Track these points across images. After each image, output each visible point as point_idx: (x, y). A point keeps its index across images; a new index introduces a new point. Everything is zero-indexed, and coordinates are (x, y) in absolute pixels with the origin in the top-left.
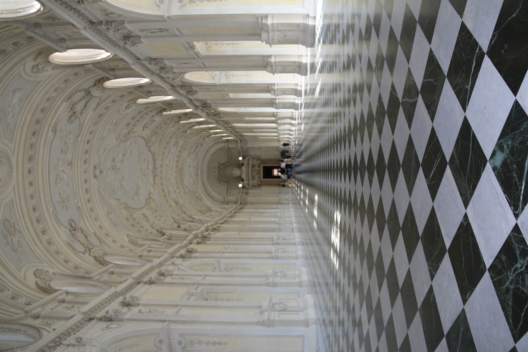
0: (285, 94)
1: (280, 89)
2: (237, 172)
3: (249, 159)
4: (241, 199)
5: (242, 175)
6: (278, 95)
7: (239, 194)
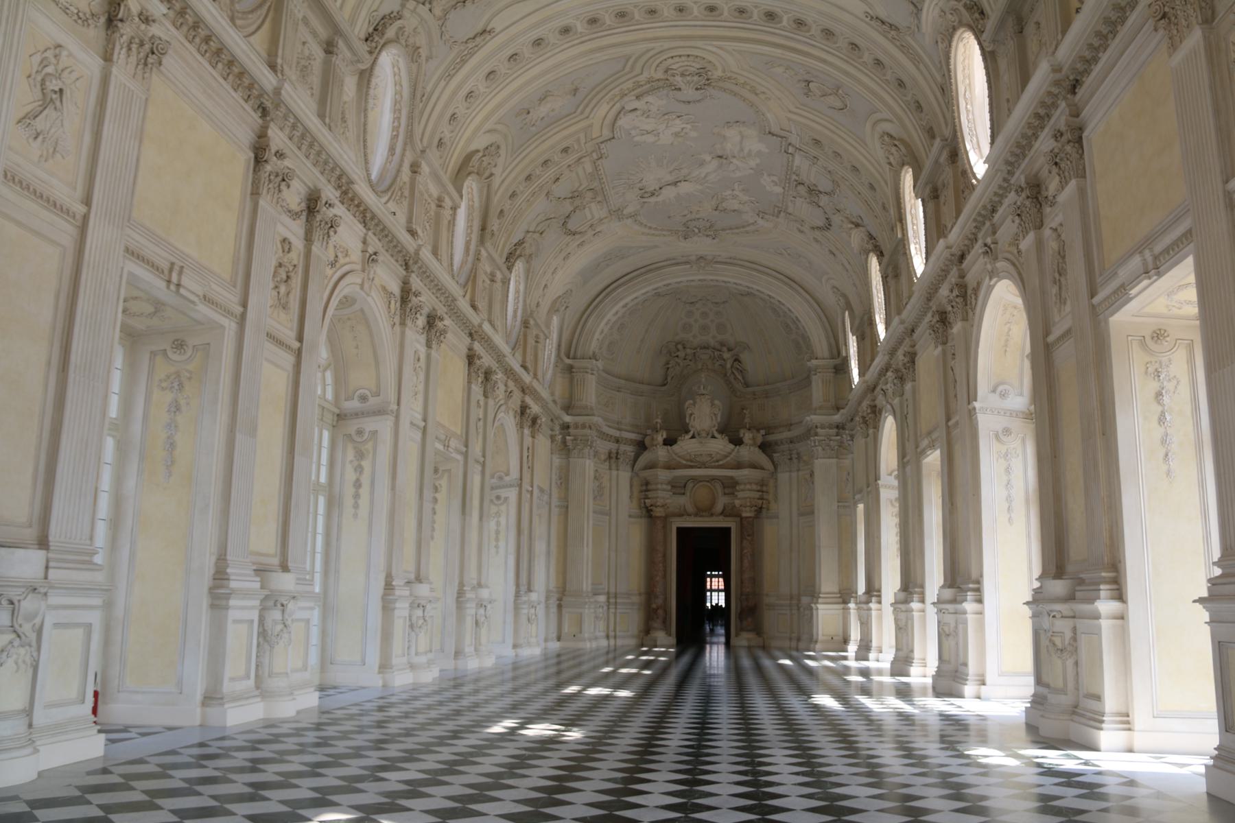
1: (965, 623)
2: (704, 415)
3: (763, 469)
4: (584, 427)
5: (693, 437)
7: (609, 426)
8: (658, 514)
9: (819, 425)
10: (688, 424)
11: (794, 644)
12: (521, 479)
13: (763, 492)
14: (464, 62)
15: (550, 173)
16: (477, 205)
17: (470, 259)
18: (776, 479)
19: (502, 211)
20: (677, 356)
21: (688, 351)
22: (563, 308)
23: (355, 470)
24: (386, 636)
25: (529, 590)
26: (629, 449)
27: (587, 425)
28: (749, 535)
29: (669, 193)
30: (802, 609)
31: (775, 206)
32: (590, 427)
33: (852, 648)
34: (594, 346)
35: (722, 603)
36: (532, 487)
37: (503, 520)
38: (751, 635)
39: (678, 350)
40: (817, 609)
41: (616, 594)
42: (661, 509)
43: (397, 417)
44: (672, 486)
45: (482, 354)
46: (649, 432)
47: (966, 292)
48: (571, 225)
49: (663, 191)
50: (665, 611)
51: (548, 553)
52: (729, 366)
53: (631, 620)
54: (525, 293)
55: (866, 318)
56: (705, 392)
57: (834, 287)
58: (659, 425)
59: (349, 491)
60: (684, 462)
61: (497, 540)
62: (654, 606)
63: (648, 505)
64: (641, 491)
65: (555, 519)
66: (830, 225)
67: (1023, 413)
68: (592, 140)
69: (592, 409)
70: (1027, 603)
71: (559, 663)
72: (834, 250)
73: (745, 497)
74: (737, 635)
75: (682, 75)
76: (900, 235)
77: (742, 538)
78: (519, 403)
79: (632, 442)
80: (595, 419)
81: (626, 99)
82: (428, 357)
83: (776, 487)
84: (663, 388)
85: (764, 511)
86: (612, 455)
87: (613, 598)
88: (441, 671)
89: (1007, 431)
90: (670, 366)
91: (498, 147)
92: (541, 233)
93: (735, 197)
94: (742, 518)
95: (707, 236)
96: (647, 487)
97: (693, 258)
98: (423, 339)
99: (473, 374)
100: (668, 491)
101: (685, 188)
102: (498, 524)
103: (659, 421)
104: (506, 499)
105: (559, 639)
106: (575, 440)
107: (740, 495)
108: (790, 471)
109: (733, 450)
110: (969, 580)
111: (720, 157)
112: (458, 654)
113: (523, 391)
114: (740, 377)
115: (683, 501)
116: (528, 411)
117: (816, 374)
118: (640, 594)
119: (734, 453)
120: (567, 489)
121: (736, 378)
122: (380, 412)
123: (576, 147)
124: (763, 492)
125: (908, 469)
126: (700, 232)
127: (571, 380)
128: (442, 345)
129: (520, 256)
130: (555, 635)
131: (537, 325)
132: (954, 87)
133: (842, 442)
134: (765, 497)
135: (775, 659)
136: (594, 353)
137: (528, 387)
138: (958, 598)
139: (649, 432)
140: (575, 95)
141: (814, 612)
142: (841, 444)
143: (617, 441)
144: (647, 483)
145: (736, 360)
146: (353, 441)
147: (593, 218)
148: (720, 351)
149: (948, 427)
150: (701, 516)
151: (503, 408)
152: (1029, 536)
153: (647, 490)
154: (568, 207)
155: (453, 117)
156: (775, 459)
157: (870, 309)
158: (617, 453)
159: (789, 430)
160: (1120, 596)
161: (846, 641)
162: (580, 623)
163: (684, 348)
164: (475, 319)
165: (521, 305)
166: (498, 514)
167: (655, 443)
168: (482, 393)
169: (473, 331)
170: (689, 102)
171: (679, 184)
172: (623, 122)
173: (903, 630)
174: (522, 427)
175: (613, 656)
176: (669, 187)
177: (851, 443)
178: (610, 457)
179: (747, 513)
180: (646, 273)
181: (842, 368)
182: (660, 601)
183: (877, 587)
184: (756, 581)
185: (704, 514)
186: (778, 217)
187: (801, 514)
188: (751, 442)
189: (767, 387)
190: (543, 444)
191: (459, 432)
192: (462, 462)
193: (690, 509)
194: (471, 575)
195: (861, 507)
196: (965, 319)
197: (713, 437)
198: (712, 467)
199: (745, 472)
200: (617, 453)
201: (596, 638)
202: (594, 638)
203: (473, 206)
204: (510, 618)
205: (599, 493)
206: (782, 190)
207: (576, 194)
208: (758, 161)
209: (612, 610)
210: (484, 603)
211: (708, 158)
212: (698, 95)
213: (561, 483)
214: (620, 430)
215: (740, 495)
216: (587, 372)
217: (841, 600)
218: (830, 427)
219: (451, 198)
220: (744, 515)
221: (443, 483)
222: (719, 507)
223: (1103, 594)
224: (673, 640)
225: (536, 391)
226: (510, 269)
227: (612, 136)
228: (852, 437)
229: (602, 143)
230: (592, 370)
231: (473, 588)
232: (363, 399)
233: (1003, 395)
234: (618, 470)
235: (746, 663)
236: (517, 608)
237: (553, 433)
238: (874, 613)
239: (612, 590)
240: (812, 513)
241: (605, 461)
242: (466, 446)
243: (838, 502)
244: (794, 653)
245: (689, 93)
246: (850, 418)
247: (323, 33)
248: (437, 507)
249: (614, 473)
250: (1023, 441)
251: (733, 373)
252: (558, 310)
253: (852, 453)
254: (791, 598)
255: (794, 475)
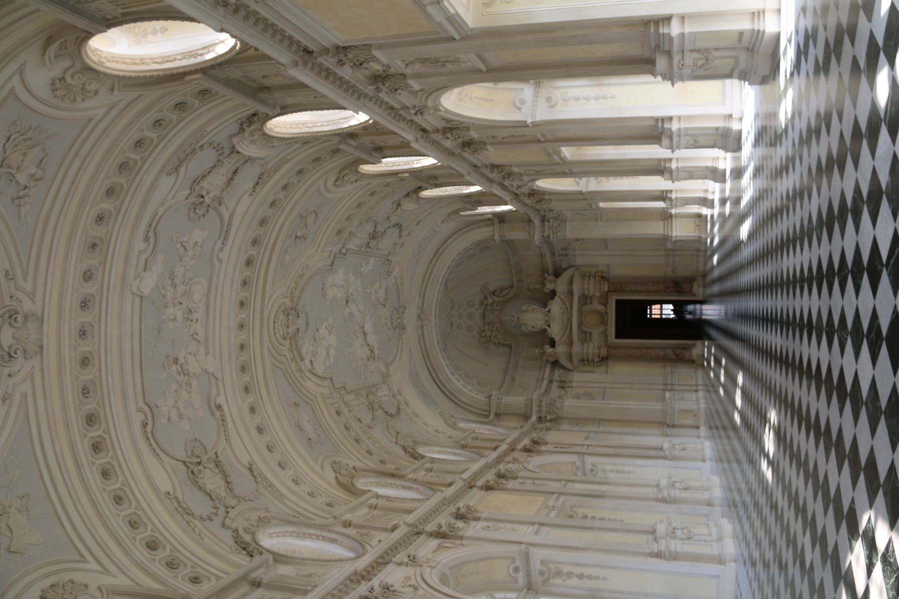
0: (696, 145)
1: (686, 129)
2: (533, 318)
3: (573, 276)
4: (540, 406)
5: (549, 326)
6: (678, 147)
7: (541, 387)
8: (606, 352)
9: (542, 235)
10: (540, 329)
11: (701, 254)
12: (578, 453)
13: (590, 276)
14: (271, 485)
15: (354, 425)
16: (375, 480)
17: (415, 486)
18: (581, 266)
19: (381, 461)
20: (490, 336)
21: (486, 328)
22: (453, 419)
23: (570, 577)
24: (697, 558)
25: (661, 449)
26: (558, 373)
27: (539, 403)
28: (622, 286)
29: (372, 339)
30: (676, 248)
31: (384, 263)
32: (541, 401)
33: (705, 211)
34: (481, 397)
35: (671, 307)
36: (584, 445)
37: (609, 467)
38: (695, 286)
39: (486, 336)
40: (676, 237)
41: (664, 384)
42: (602, 351)
43: (531, 544)
44: (585, 341)
45: (486, 479)
46: (545, 358)
47: (449, 128)
48: (393, 411)
49: (370, 343)
50: (678, 348)
51: (633, 434)
52: (497, 299)
53: (683, 373)
54: (441, 446)
55: (465, 200)
56: (516, 316)
57: (443, 222)
58: (541, 351)
59: (586, 583)
60: (567, 333)
61: (623, 472)
62: (673, 356)
63: (598, 360)
64: (588, 365)
65: (608, 429)
66: (398, 224)
67: (535, 88)
68: (331, 394)
69: (527, 400)
70: (673, 84)
71: (717, 428)
72: (417, 221)
73: (593, 288)
74: (695, 295)
75: (288, 327)
76: (407, 175)
77: (623, 291)
78: (522, 453)
79: (552, 371)
80: (535, 397)
81: (303, 368)
82: (486, 520)
83: (586, 266)
84: (513, 347)
85: (604, 275)
86: (562, 386)
87: (667, 387)
88: (723, 517)
89: (548, 99)
90: (497, 342)
91: (334, 462)
92: (398, 433)
93: (376, 292)
94: (609, 291)
95: (403, 312)
96: (585, 361)
97: (419, 323)
98: (473, 523)
99: (500, 487)
100: (588, 344)
101: (368, 328)
102: (611, 471)
103: (537, 350)
104: (593, 464)
105: (698, 427)
106: (550, 412)
107: (592, 292)
108: (575, 255)
109: (559, 297)
110: (655, 127)
111: (347, 301)
112: (709, 504)
113: (513, 450)
114: (506, 291)
115: (596, 334)
116: (528, 447)
117: (505, 237)
118: (665, 367)
119: (562, 296)
120: (586, 419)
121: (507, 294)
122: (527, 557)
123: (336, 406)
124: (590, 276)
125: (574, 170)
126: (400, 318)
127: (505, 414)
128: (478, 509)
129: (414, 449)
130: (695, 431)
131: (465, 438)
132: (304, 135)
133: (554, 218)
134: (594, 274)
135: (713, 267)
136: (486, 397)
137: (511, 446)
138: (669, 134)
139: (545, 358)
140: (298, 405)
141: (678, 239)
142: (556, 219)
143: (551, 381)
144: (583, 360)
145: (494, 294)
146: (548, 579)
147: (388, 395)
148: (486, 305)
149: (545, 142)
150: (607, 321)
151: (526, 465)
152: (623, 84)
153: (588, 360)
154: (379, 413)
155: (311, 494)
156: (566, 266)
157: (459, 197)
158: (560, 382)
159: (545, 256)
160: (667, 19)
161: (699, 216)
162: (686, 412)
163: (484, 331)
164: (459, 484)
165: (450, 450)
166: (604, 471)
167: (553, 354)
168: (514, 480)
169: (468, 486)
170: (307, 323)
171: (365, 332)
172: (320, 371)
173: (692, 174)
174: (540, 452)
175: (711, 387)
176: (367, 339)
177: (555, 212)
178: (563, 387)
179: (605, 287)
180: (429, 358)
181: (501, 218)
182: (670, 352)
183: (660, 193)
184: (655, 281)
185: (605, 318)
186: (391, 262)
187: (607, 248)
188: (553, 284)
189: (514, 272)
190: (552, 436)
191: (543, 499)
192: (566, 497)
193: (601, 329)
194: (650, 492)
195: (602, 205)
196: (468, 129)
197: (549, 311)
198: (571, 312)
199: (576, 289)
200: (560, 382)
201: (697, 400)
202: (698, 401)
203: (377, 483)
204: (683, 464)
205: (590, 396)
206: (373, 258)
207: (370, 407)
208: (351, 275)
209: (677, 387)
210: (671, 483)
211: (347, 311)
212: (302, 316)
213: (582, 423)
214: (543, 380)
215: (592, 292)
216: (500, 403)
217: (669, 220)
218: (543, 226)
219: (371, 498)
220: (606, 289)
221: (580, 511)
222: (601, 308)
223: (666, 31)
224: (699, 343)
225: (513, 441)
226: (423, 457)
227: (329, 380)
228: (551, 210)
229: (334, 386)
230: (498, 399)
231: (660, 490)
232: (516, 569)
233: (523, 102)
234: (572, 382)
235: (716, 288)
236: (674, 458)
237: (545, 428)
238: (679, 195)
239: (661, 387)
240: (605, 240)
241: (565, 391)
242: (553, 493)
243: (598, 221)
244: (709, 253)
245: (301, 322)
246: (537, 212)
247: (245, 588)
248: (599, 516)
249: (574, 384)
250: (555, 88)
251: (503, 296)
252: (454, 423)
253: (562, 211)
254: (668, 255)
255: (577, 253)
